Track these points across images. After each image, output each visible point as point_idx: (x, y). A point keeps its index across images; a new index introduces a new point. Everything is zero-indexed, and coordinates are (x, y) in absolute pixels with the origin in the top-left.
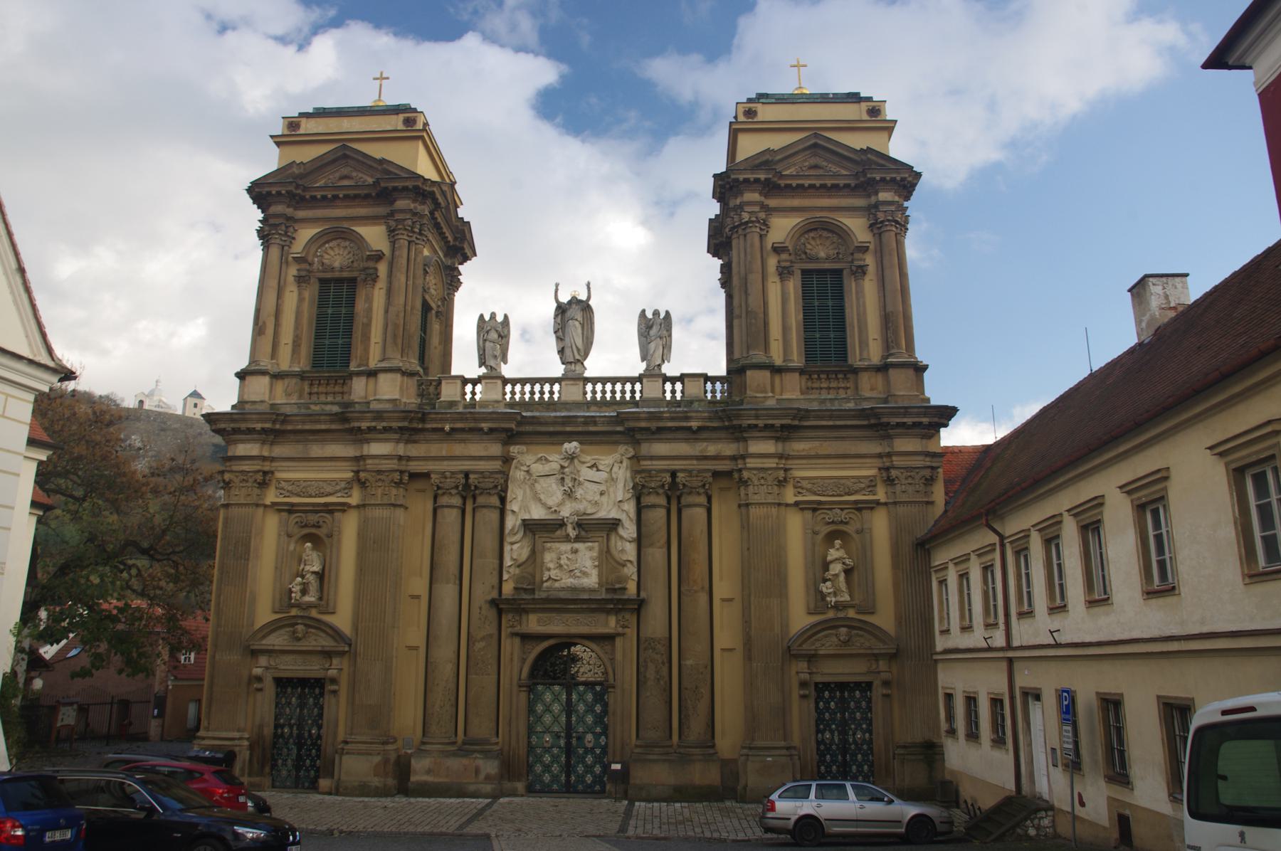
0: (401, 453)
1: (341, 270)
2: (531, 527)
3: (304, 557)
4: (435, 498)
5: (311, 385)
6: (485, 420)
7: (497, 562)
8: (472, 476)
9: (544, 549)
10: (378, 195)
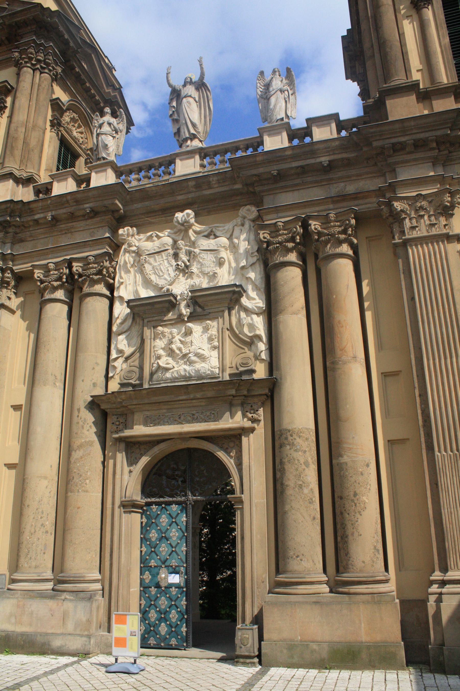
8: (74, 264)
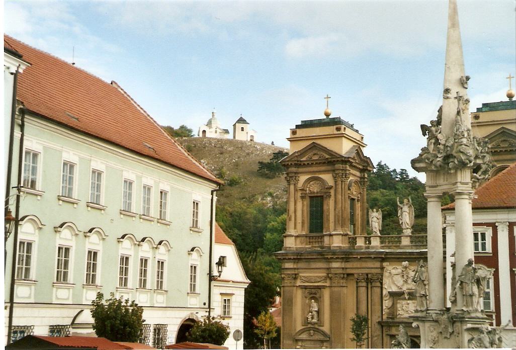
0: (343, 267)
1: (317, 193)
2: (392, 294)
3: (312, 305)
4: (357, 284)
5: (310, 238)
6: (372, 254)
7: (381, 307)
8: (369, 275)
9: (397, 303)
10: (328, 162)
